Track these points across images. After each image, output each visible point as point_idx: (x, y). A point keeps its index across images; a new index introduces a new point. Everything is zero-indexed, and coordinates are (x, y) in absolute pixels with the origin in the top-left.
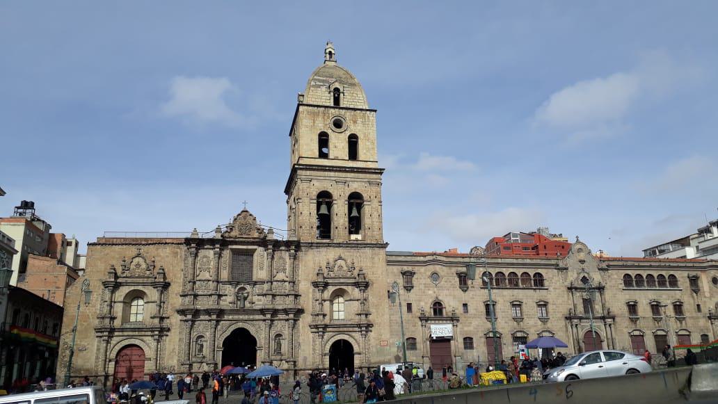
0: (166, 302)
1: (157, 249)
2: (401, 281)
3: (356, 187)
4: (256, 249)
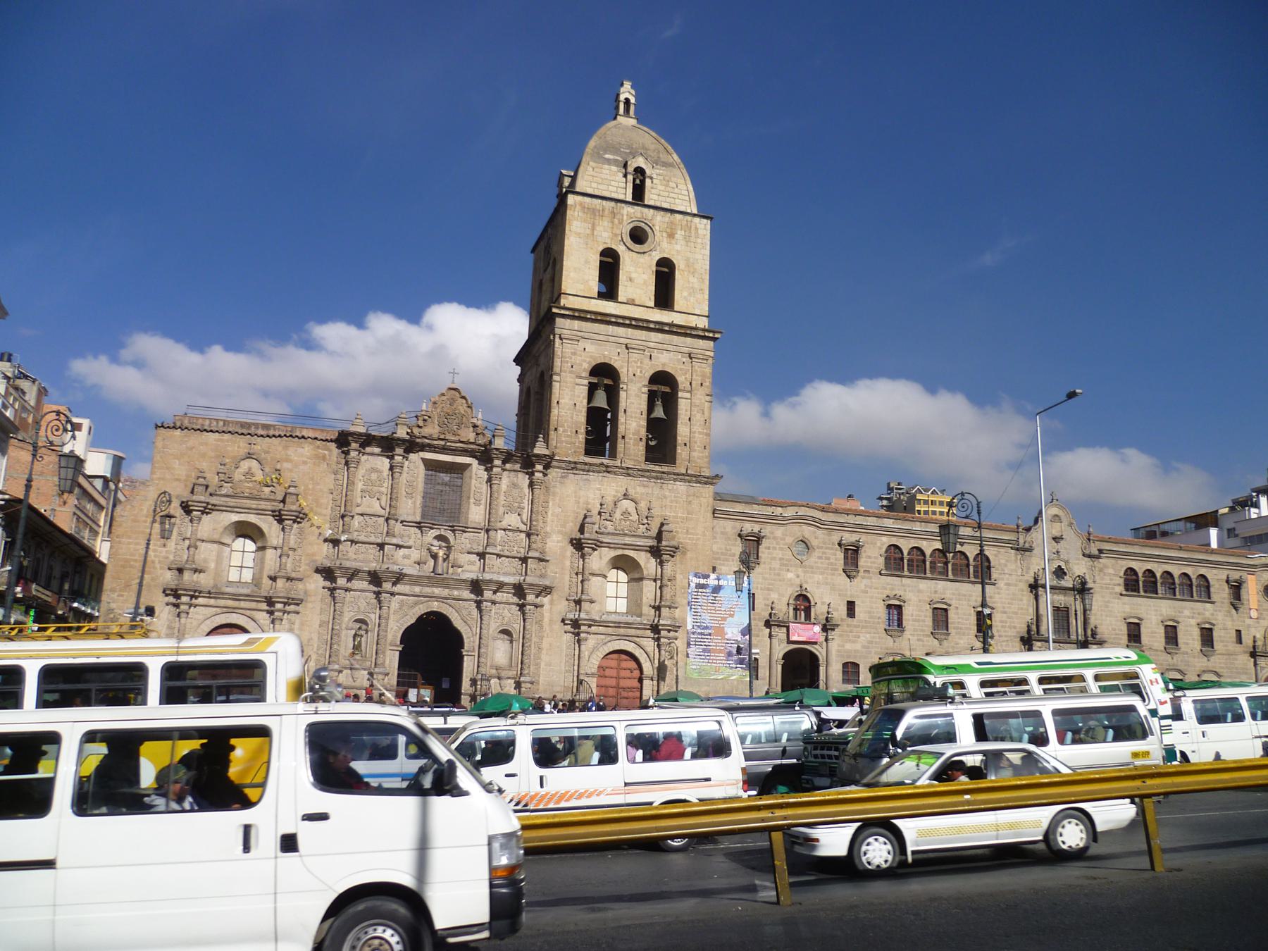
0: (299, 552)
1: (286, 447)
2: (737, 548)
4: (470, 465)
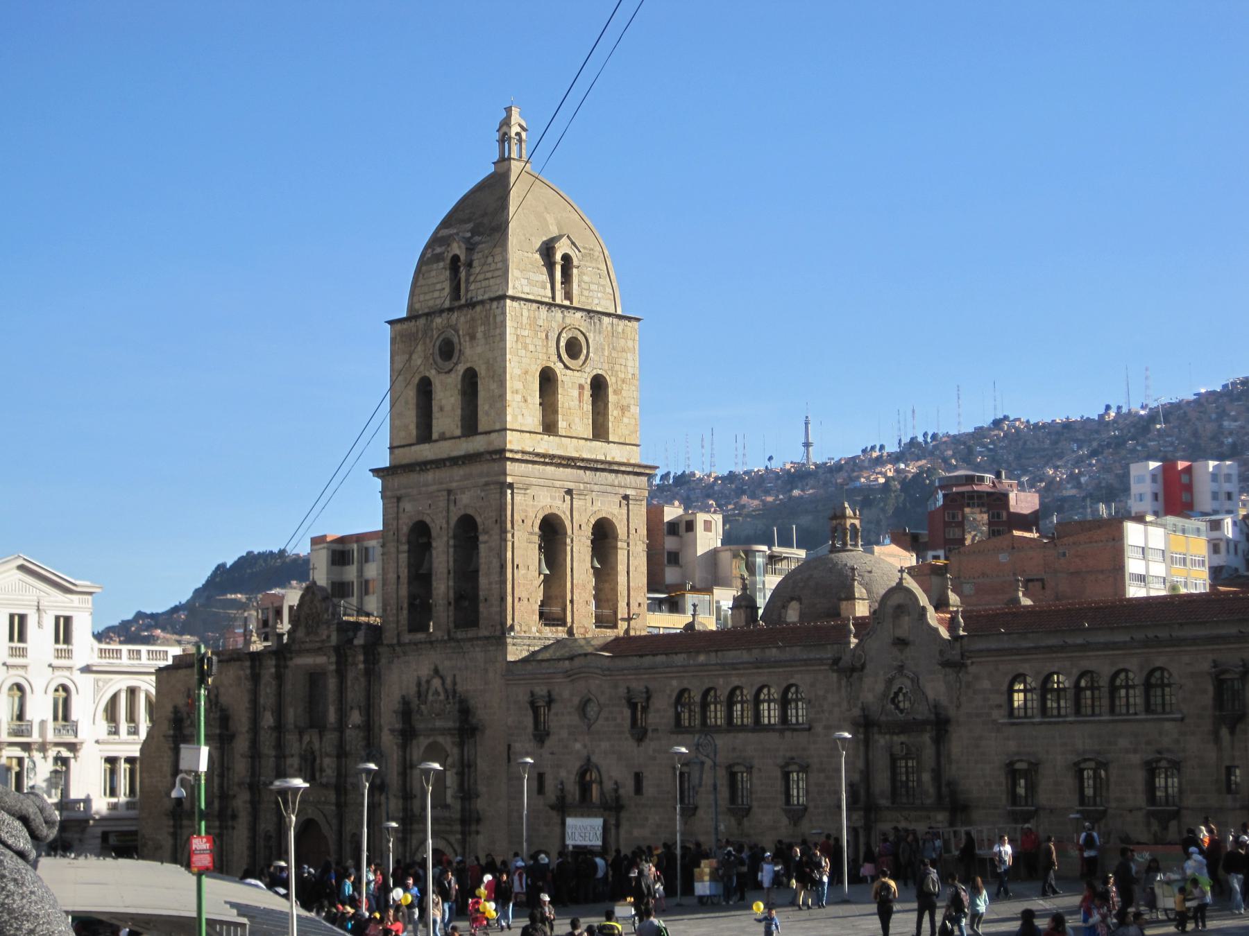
2: (529, 721)
3: (467, 501)
